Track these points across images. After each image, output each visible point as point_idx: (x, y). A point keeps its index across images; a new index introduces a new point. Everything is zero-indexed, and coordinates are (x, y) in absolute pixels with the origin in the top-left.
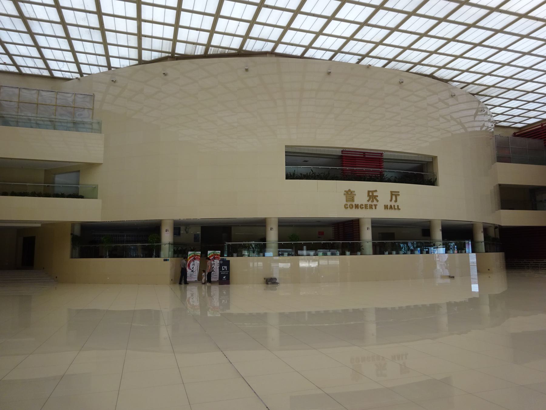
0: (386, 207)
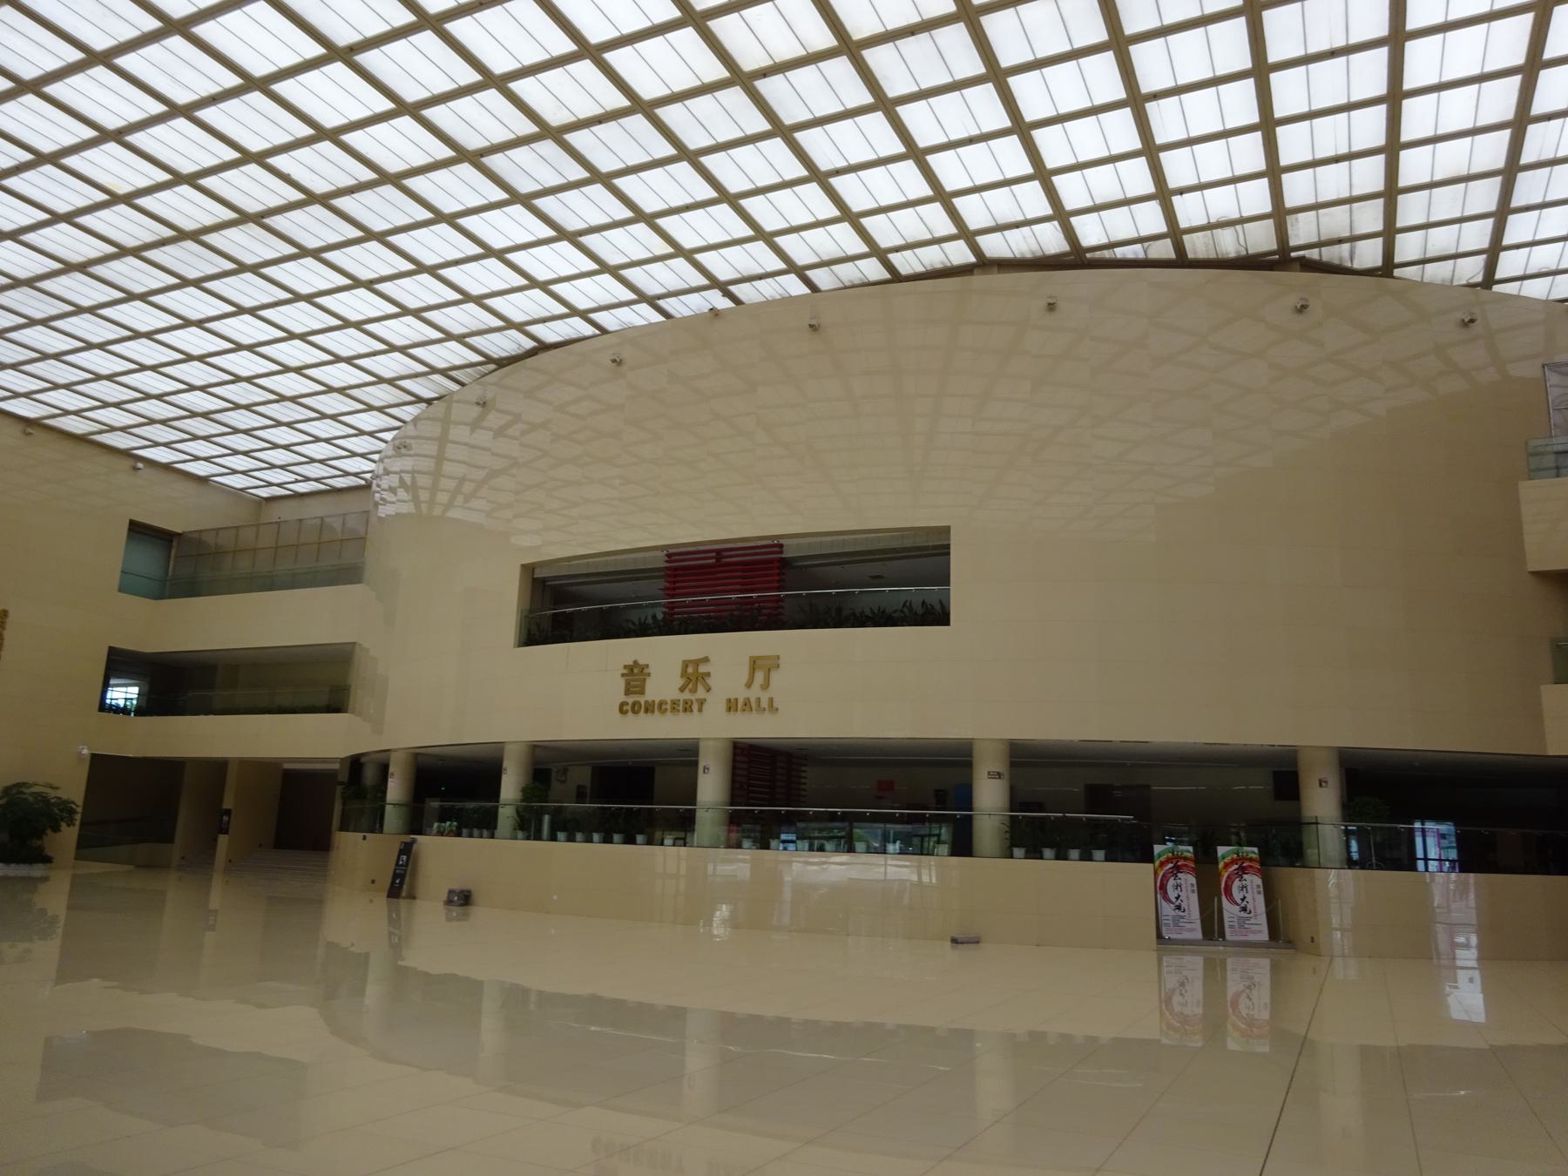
0: (731, 706)
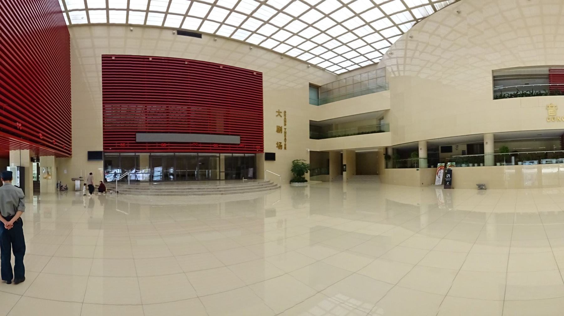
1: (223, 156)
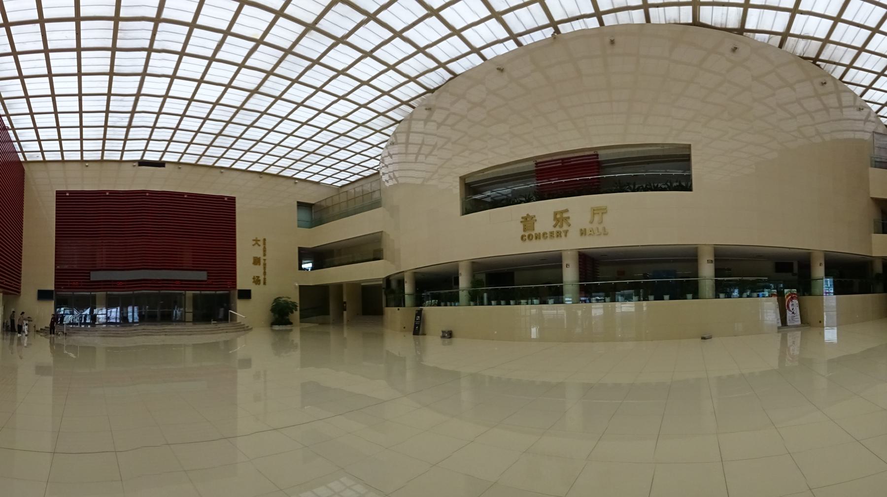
0: (583, 232)
1: (190, 293)
